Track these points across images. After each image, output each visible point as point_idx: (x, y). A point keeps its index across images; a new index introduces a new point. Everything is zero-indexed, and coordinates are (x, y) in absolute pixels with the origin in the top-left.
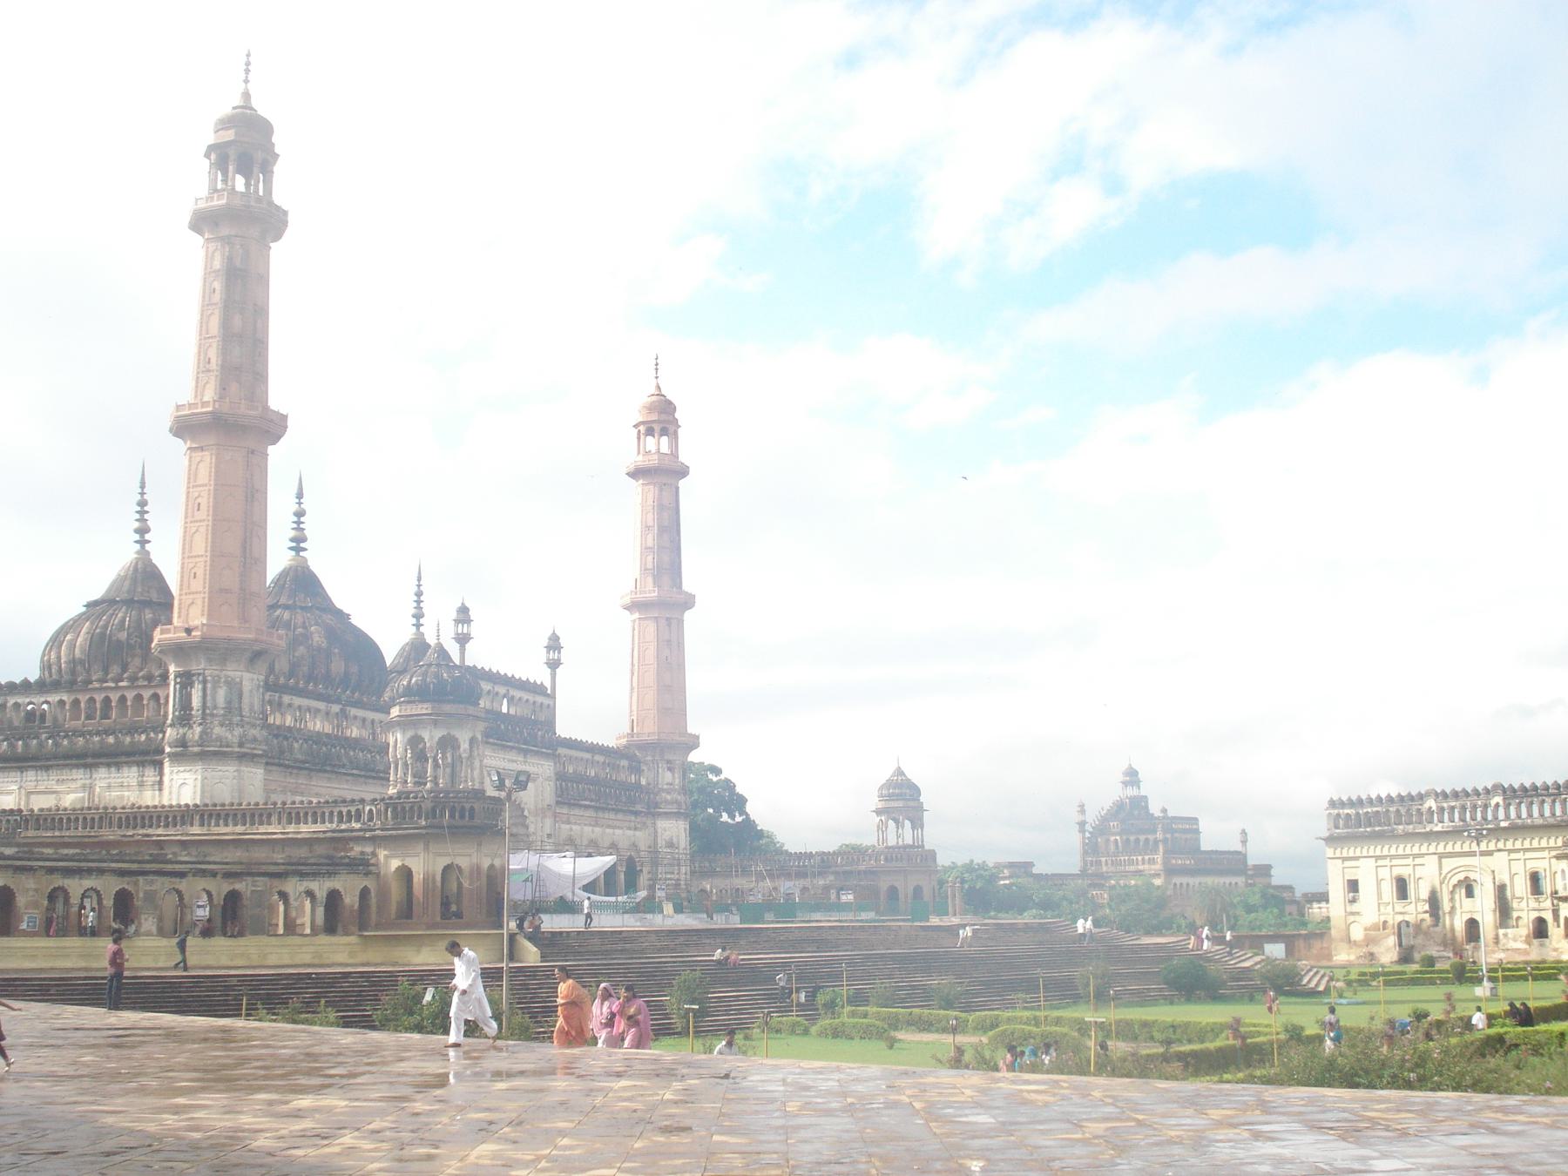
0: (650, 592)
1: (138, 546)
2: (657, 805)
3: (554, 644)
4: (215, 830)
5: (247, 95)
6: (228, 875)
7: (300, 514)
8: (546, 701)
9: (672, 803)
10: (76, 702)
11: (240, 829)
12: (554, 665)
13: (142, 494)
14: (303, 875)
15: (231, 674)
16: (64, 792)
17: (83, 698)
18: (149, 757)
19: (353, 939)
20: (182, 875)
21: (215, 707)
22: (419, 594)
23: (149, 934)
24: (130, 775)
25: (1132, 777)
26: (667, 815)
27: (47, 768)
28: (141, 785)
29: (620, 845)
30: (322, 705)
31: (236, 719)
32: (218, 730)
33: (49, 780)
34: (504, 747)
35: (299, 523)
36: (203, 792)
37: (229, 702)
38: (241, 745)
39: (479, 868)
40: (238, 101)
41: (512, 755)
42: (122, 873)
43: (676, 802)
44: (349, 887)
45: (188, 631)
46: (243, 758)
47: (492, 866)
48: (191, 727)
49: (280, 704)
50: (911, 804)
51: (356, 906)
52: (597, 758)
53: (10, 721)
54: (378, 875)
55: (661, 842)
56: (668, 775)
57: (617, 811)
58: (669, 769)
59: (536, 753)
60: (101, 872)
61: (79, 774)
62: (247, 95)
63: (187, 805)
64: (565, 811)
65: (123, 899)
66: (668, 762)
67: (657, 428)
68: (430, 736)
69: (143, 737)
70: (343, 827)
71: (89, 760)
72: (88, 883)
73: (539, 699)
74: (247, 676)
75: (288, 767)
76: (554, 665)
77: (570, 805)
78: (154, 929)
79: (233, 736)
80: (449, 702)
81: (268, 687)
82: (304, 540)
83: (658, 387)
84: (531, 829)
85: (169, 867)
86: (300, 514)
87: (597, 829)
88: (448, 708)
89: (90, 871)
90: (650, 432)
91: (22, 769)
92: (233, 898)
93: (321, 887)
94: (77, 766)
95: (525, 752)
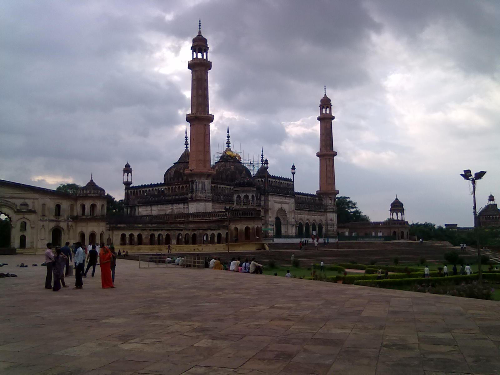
0: (325, 152)
1: (186, 148)
2: (327, 210)
3: (293, 168)
4: (195, 219)
5: (200, 32)
6: (193, 230)
8: (291, 183)
9: (332, 208)
10: (169, 188)
11: (200, 219)
12: (293, 173)
13: (186, 135)
14: (211, 230)
15: (202, 180)
16: (168, 209)
17: (170, 187)
18: (185, 201)
19: (225, 245)
20: (182, 230)
21: (199, 189)
23: (174, 244)
24: (181, 206)
25: (491, 198)
26: (330, 212)
27: (163, 204)
28: (184, 208)
29: (317, 221)
30: (229, 187)
31: (204, 191)
32: (199, 194)
33: (164, 207)
34: (279, 195)
35: (228, 139)
36: (197, 210)
37: (202, 188)
38: (205, 198)
39: (254, 227)
40: (197, 35)
42: (167, 230)
44: (223, 233)
45: (191, 170)
46: (206, 201)
47: (258, 227)
48: (193, 194)
49: (217, 187)
50: (400, 208)
51: (225, 237)
52: (308, 197)
53: (155, 193)
54: (230, 229)
55: (328, 219)
56: (330, 202)
58: (331, 200)
60: (162, 230)
61: (170, 206)
62: (200, 32)
63: (155, 215)
65: (168, 236)
66: (330, 198)
67: (325, 107)
68: (242, 195)
69: (184, 196)
70: (223, 218)
71: (172, 202)
72: (159, 232)
73: (289, 183)
74: (206, 180)
75: (219, 202)
76: (293, 173)
77: (300, 210)
78: (176, 243)
79: (203, 196)
80: (246, 187)
81: (212, 183)
82: (230, 144)
83: (325, 95)
84: (288, 216)
85: (179, 228)
86: (228, 137)
87: (309, 216)
88: (246, 188)
89: (160, 230)
90: (323, 108)
91: (157, 205)
92: (194, 235)
93: (216, 233)
94: (170, 204)
95: (286, 197)
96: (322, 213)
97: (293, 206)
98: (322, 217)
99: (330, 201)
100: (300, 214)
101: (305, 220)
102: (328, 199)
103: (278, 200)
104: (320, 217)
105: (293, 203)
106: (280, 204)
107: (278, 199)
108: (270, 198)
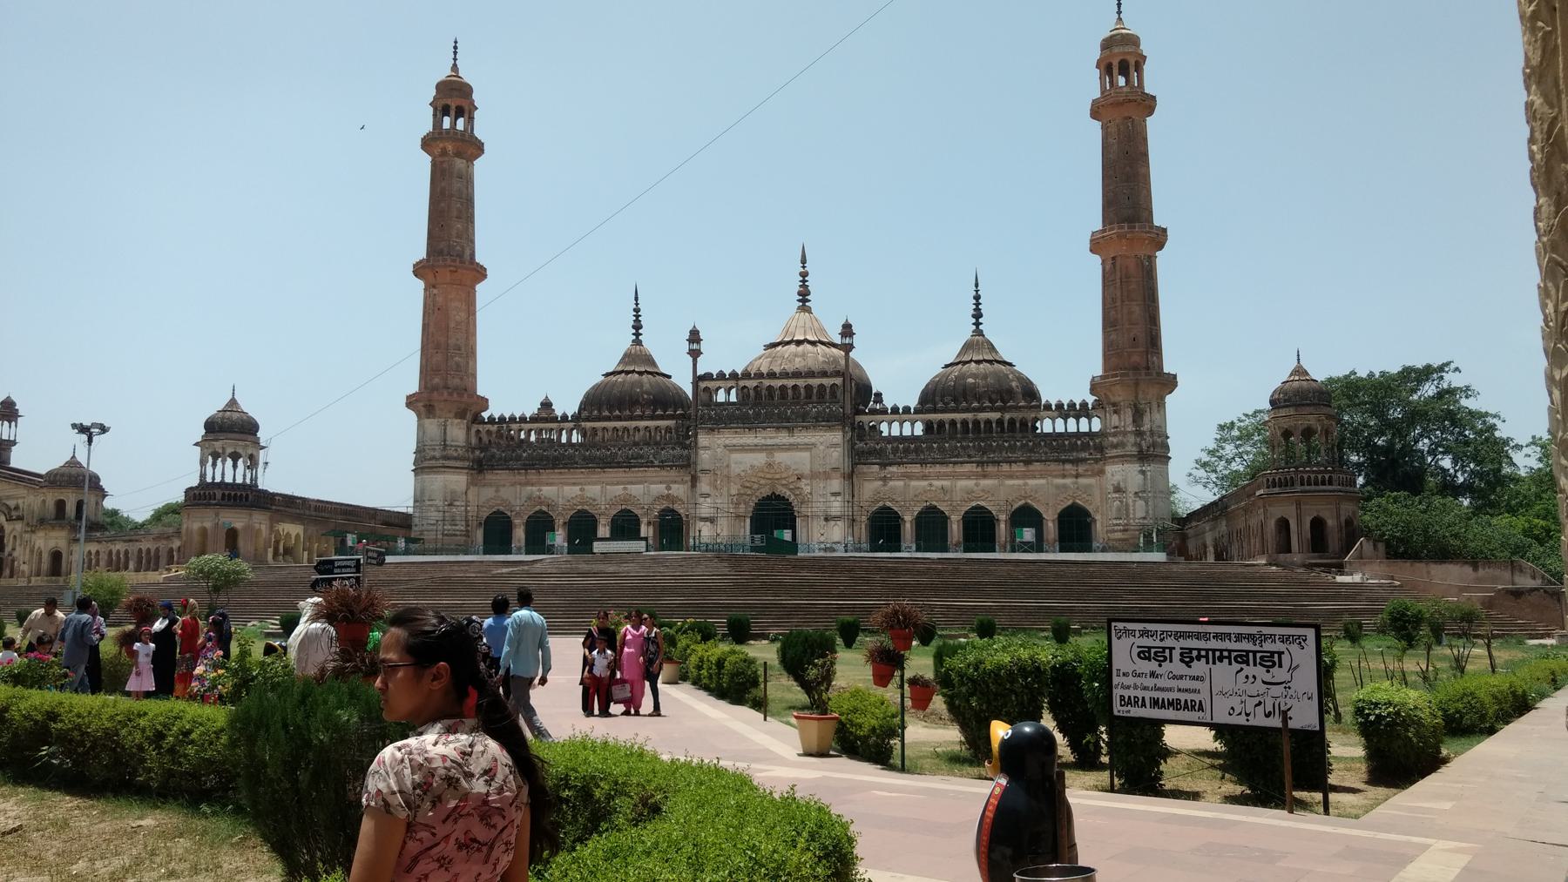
3: (847, 330)
5: (455, 67)
7: (804, 275)
12: (848, 348)
22: (977, 298)
35: (804, 281)
41: (770, 433)
43: (1121, 445)
56: (1115, 420)
57: (1028, 462)
59: (807, 428)
62: (455, 67)
64: (916, 469)
66: (1114, 405)
77: (923, 463)
84: (807, 489)
86: (804, 275)
95: (790, 430)
96: (1081, 469)
97: (835, 455)
98: (1082, 481)
99: (1115, 417)
100: (924, 477)
101: (957, 497)
102: (1109, 409)
103: (756, 441)
104: (1068, 481)
105: (835, 445)
106: (763, 455)
107: (749, 439)
108: (703, 439)
